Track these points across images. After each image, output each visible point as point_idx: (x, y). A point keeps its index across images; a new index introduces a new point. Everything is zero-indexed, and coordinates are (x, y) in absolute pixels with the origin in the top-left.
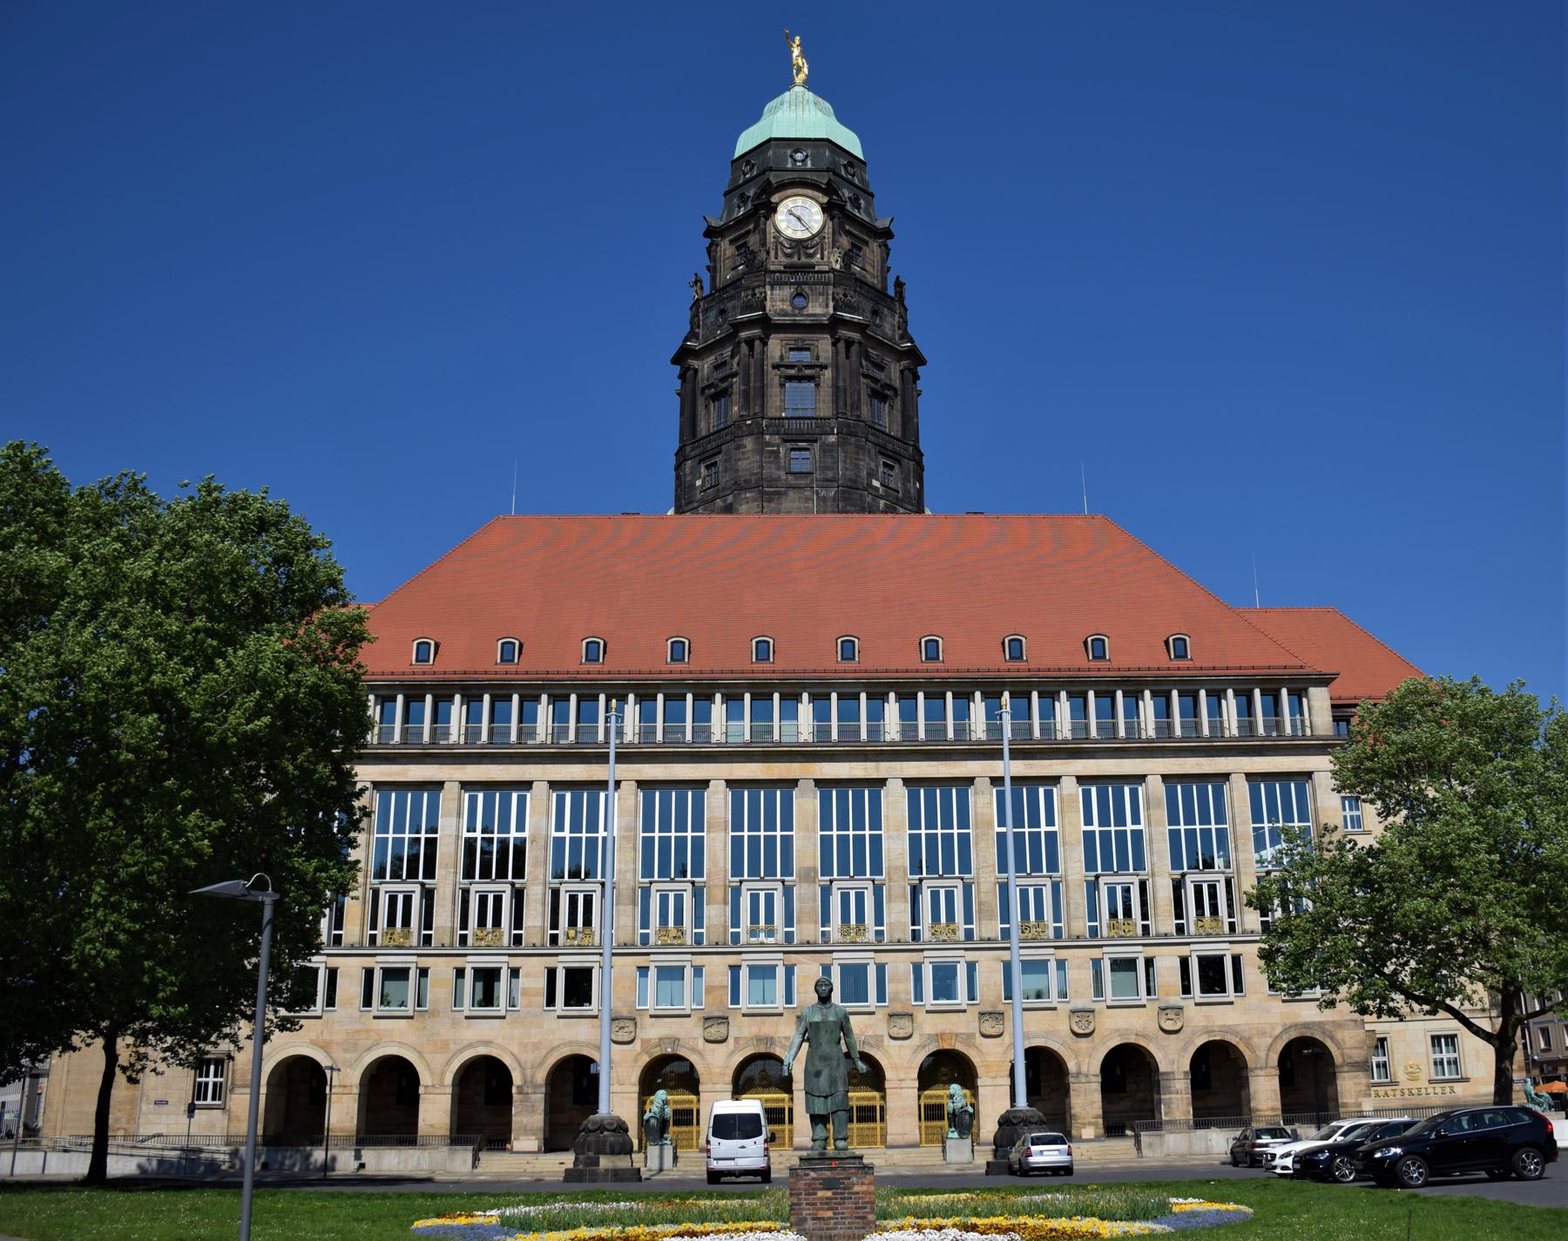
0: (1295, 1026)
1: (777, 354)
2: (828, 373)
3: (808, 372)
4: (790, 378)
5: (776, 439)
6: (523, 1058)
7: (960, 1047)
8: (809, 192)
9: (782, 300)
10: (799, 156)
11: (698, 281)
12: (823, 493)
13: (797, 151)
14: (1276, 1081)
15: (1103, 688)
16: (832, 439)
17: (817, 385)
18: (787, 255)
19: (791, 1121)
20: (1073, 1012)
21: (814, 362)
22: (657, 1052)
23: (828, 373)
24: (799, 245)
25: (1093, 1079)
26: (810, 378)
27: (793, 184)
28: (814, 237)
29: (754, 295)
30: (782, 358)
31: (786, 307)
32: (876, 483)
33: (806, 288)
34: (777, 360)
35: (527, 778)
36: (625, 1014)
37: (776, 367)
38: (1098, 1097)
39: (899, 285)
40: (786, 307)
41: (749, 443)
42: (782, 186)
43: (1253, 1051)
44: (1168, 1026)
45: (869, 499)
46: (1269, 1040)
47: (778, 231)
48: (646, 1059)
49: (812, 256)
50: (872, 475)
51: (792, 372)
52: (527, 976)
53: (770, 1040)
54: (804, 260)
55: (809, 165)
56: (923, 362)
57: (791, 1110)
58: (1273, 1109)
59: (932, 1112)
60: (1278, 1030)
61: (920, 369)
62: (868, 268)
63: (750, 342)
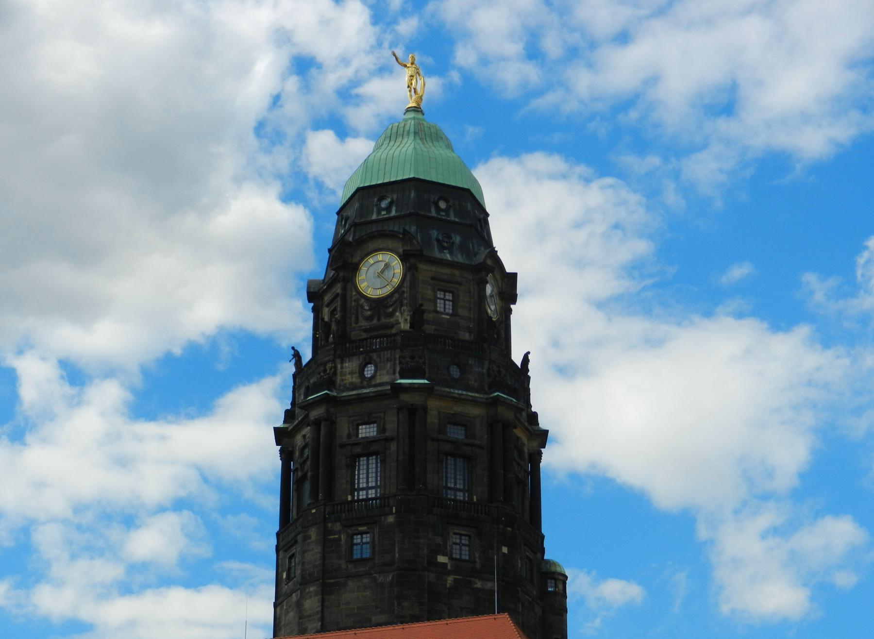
1: (345, 432)
3: (374, 448)
4: (360, 455)
5: (338, 526)
8: (390, 243)
9: (352, 373)
10: (384, 204)
12: (380, 579)
13: (381, 199)
16: (391, 519)
17: (383, 461)
18: (369, 319)
21: (383, 436)
23: (393, 446)
24: (378, 304)
26: (376, 453)
27: (372, 237)
28: (391, 295)
29: (325, 371)
30: (349, 436)
31: (355, 379)
32: (442, 559)
33: (374, 356)
34: (345, 440)
37: (343, 446)
40: (355, 379)
41: (313, 533)
42: (360, 242)
49: (392, 314)
50: (435, 552)
51: (358, 450)
54: (384, 320)
55: (393, 213)
62: (462, 312)
63: (317, 424)
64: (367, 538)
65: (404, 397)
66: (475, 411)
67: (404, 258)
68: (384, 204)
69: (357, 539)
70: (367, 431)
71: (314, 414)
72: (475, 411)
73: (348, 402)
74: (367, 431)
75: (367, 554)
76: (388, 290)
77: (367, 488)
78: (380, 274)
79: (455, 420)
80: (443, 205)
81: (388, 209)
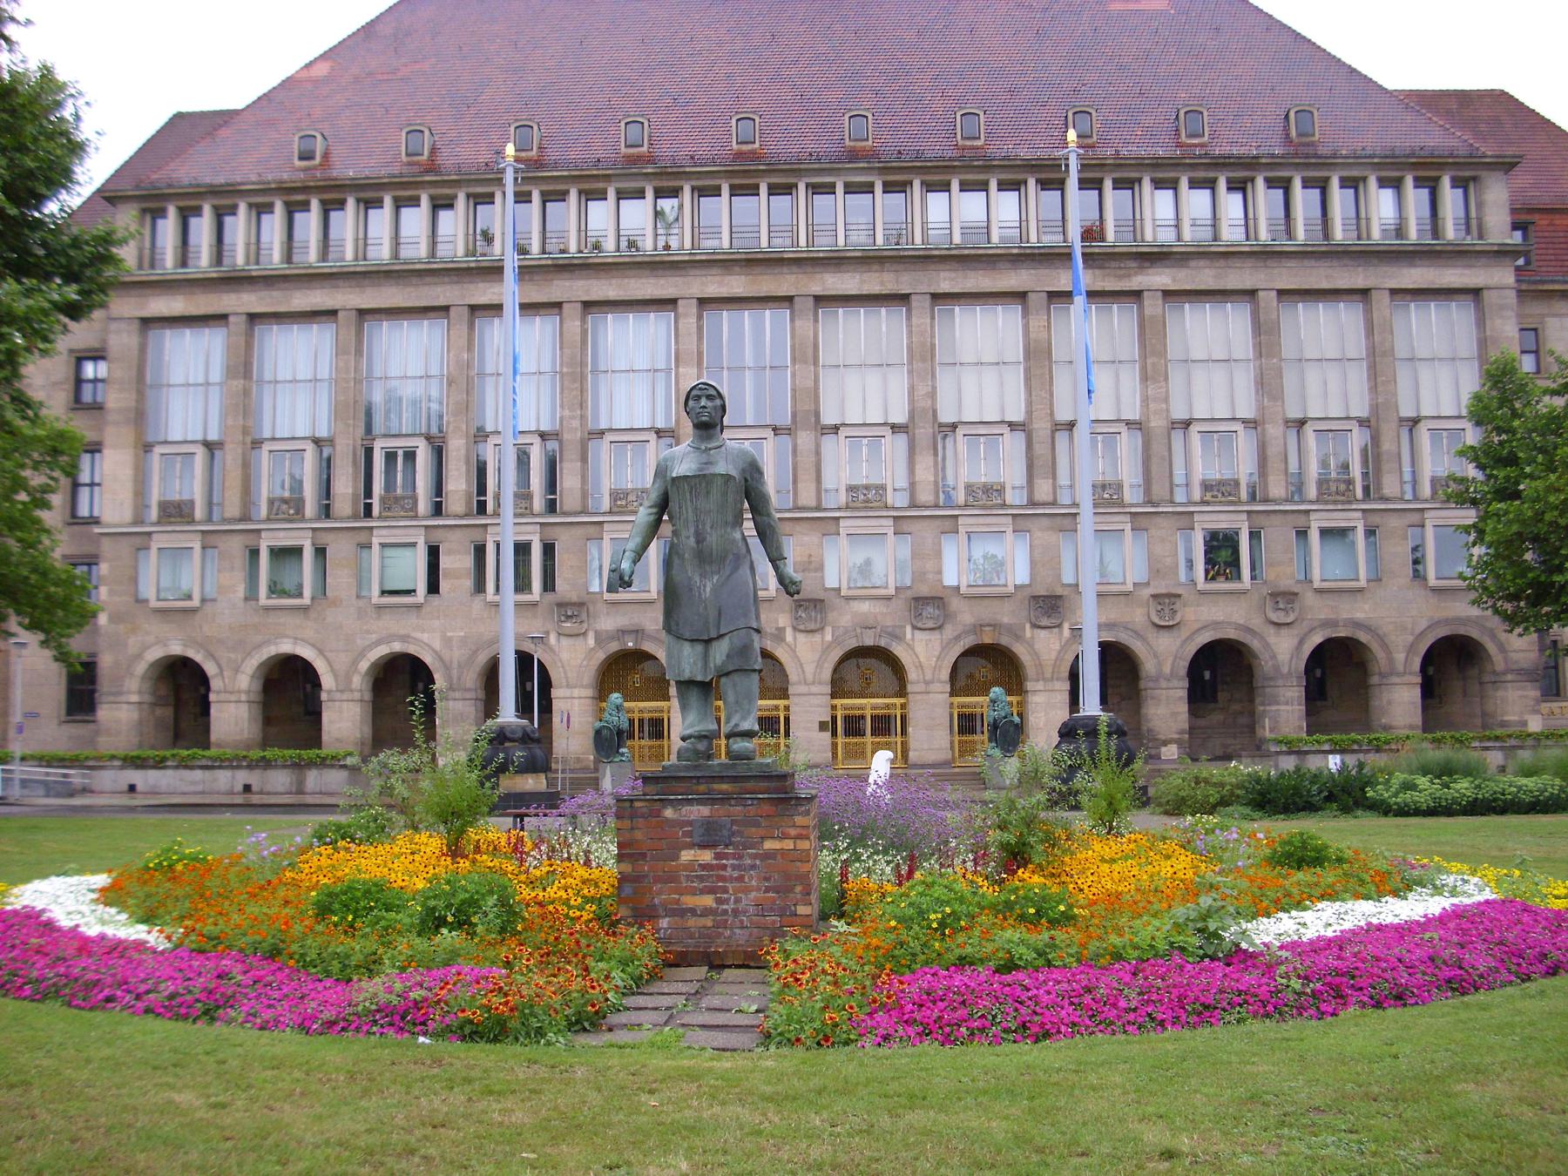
0: (1447, 622)
6: (446, 655)
7: (1005, 641)
14: (1417, 692)
15: (1201, 174)
20: (1154, 596)
22: (614, 647)
25: (1175, 683)
35: (441, 302)
36: (575, 599)
38: (1183, 708)
43: (1389, 652)
44: (1274, 616)
46: (1411, 638)
48: (601, 656)
52: (450, 552)
57: (787, 719)
58: (1411, 727)
59: (967, 723)
60: (1424, 624)
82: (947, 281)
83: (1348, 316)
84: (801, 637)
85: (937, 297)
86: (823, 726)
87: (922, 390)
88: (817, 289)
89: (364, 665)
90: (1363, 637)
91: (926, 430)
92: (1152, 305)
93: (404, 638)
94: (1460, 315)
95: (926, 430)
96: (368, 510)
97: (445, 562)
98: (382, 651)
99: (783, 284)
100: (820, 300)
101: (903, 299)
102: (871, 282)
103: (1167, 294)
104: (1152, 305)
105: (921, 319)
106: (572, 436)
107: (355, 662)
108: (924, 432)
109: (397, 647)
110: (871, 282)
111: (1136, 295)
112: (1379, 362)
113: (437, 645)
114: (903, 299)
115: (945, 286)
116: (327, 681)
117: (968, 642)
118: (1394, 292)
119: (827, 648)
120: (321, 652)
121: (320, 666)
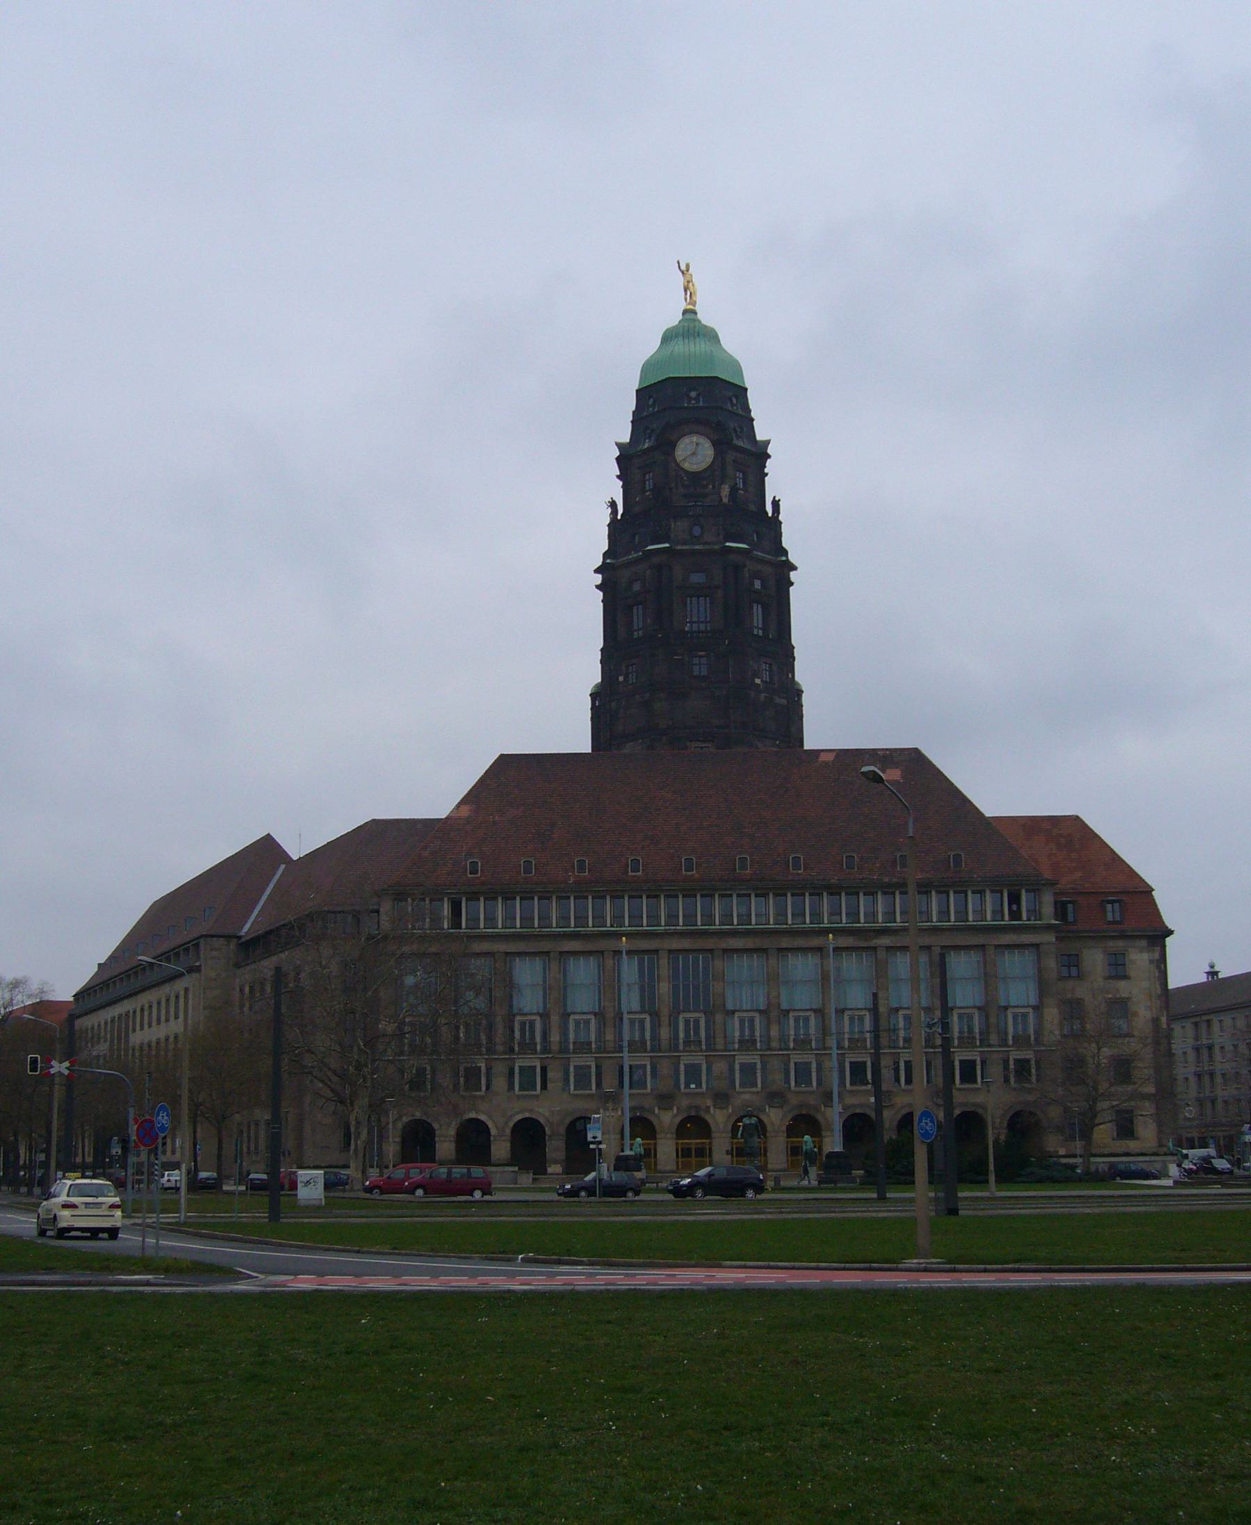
2: (720, 593)
10: (693, 394)
11: (613, 505)
19: (710, 1156)
24: (695, 476)
32: (758, 681)
39: (776, 504)
45: (752, 694)
47: (678, 465)
49: (706, 486)
53: (697, 1108)
56: (794, 568)
59: (795, 1151)
61: (793, 575)
64: (704, 660)
65: (731, 557)
66: (768, 570)
67: (715, 444)
68: (693, 394)
69: (696, 661)
70: (697, 578)
71: (656, 560)
72: (768, 570)
73: (681, 554)
74: (697, 578)
75: (704, 672)
76: (704, 466)
77: (699, 622)
78: (694, 452)
79: (757, 575)
80: (734, 401)
81: (697, 399)
82: (785, 943)
83: (975, 957)
84: (718, 1111)
85: (780, 950)
86: (727, 1152)
87: (774, 994)
88: (724, 945)
89: (511, 1124)
90: (980, 1111)
91: (774, 1013)
92: (882, 954)
93: (531, 1111)
94: (1029, 957)
95: (774, 1013)
96: (512, 1050)
97: (550, 1075)
98: (520, 1117)
99: (710, 943)
100: (725, 951)
101: (765, 951)
102: (749, 943)
103: (889, 948)
104: (882, 954)
105: (772, 961)
106: (610, 1014)
107: (506, 1123)
108: (774, 1014)
109: (527, 1115)
110: (749, 943)
111: (875, 948)
112: (988, 979)
113: (547, 1114)
114: (765, 951)
115: (784, 945)
116: (493, 1131)
117: (796, 1112)
118: (997, 946)
119: (730, 1116)
120: (490, 1117)
121: (490, 1124)
